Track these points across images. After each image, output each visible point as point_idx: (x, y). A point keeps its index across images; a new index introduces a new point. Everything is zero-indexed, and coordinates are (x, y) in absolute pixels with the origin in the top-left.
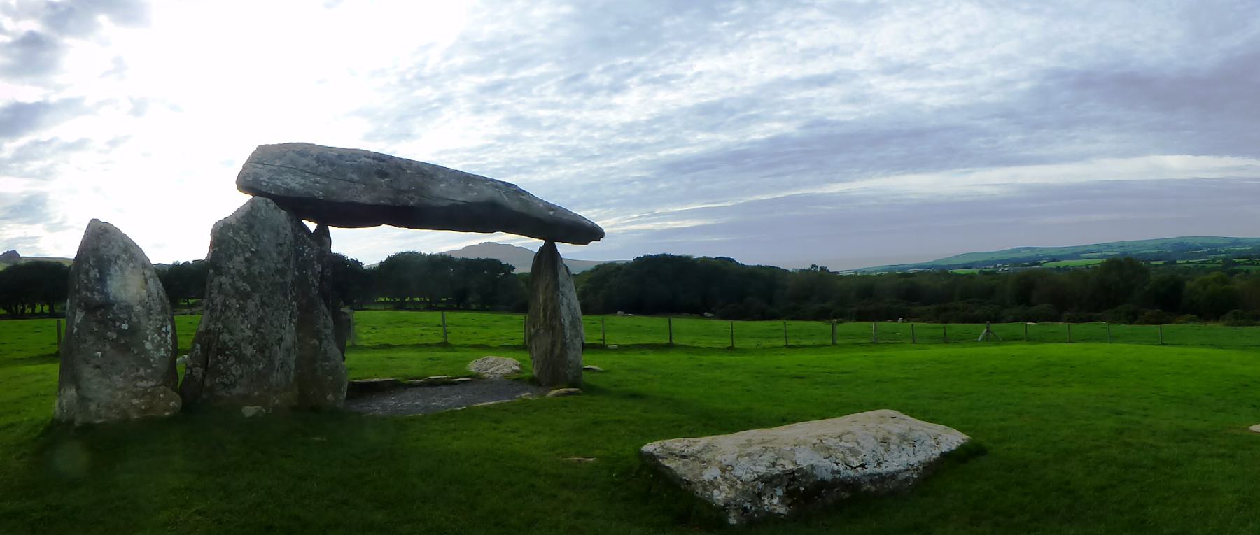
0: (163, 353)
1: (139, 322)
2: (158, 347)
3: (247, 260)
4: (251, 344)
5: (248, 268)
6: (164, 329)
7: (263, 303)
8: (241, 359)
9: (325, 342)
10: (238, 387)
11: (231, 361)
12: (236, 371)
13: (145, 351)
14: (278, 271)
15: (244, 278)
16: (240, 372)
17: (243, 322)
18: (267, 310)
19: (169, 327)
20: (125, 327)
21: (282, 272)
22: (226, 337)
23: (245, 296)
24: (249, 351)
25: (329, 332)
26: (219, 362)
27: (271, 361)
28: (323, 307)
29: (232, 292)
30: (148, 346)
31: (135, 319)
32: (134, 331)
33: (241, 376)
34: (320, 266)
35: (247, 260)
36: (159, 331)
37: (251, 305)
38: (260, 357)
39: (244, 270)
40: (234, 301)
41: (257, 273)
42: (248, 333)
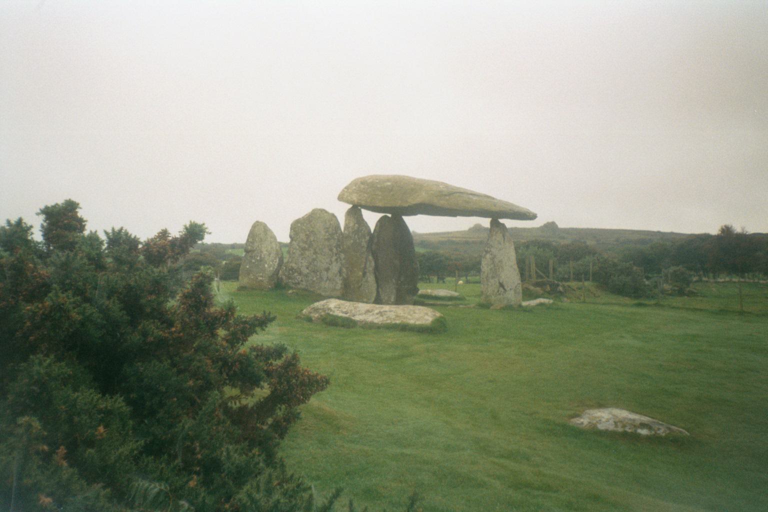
0: (271, 269)
1: (264, 258)
2: (270, 267)
3: (306, 235)
4: (307, 268)
5: (307, 238)
6: (275, 261)
7: (315, 253)
8: (300, 274)
9: (368, 274)
10: (300, 285)
11: (296, 274)
12: (299, 278)
13: (264, 266)
14: (326, 240)
15: (305, 242)
16: (300, 279)
17: (302, 259)
18: (319, 256)
19: (277, 260)
20: (258, 258)
21: (328, 240)
22: (294, 265)
23: (304, 249)
24: (306, 271)
25: (371, 269)
26: (289, 274)
27: (321, 278)
28: (371, 258)
29: (298, 247)
30: (266, 266)
31: (263, 256)
32: (261, 260)
33: (302, 281)
34: (368, 237)
35: (306, 235)
36: (273, 261)
37: (307, 253)
38: (312, 274)
39: (305, 239)
40: (298, 251)
41: (312, 240)
42: (305, 264)
